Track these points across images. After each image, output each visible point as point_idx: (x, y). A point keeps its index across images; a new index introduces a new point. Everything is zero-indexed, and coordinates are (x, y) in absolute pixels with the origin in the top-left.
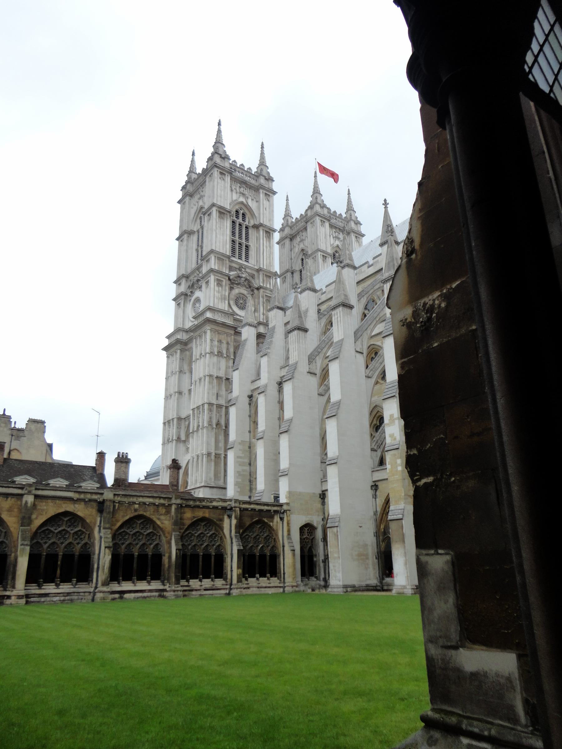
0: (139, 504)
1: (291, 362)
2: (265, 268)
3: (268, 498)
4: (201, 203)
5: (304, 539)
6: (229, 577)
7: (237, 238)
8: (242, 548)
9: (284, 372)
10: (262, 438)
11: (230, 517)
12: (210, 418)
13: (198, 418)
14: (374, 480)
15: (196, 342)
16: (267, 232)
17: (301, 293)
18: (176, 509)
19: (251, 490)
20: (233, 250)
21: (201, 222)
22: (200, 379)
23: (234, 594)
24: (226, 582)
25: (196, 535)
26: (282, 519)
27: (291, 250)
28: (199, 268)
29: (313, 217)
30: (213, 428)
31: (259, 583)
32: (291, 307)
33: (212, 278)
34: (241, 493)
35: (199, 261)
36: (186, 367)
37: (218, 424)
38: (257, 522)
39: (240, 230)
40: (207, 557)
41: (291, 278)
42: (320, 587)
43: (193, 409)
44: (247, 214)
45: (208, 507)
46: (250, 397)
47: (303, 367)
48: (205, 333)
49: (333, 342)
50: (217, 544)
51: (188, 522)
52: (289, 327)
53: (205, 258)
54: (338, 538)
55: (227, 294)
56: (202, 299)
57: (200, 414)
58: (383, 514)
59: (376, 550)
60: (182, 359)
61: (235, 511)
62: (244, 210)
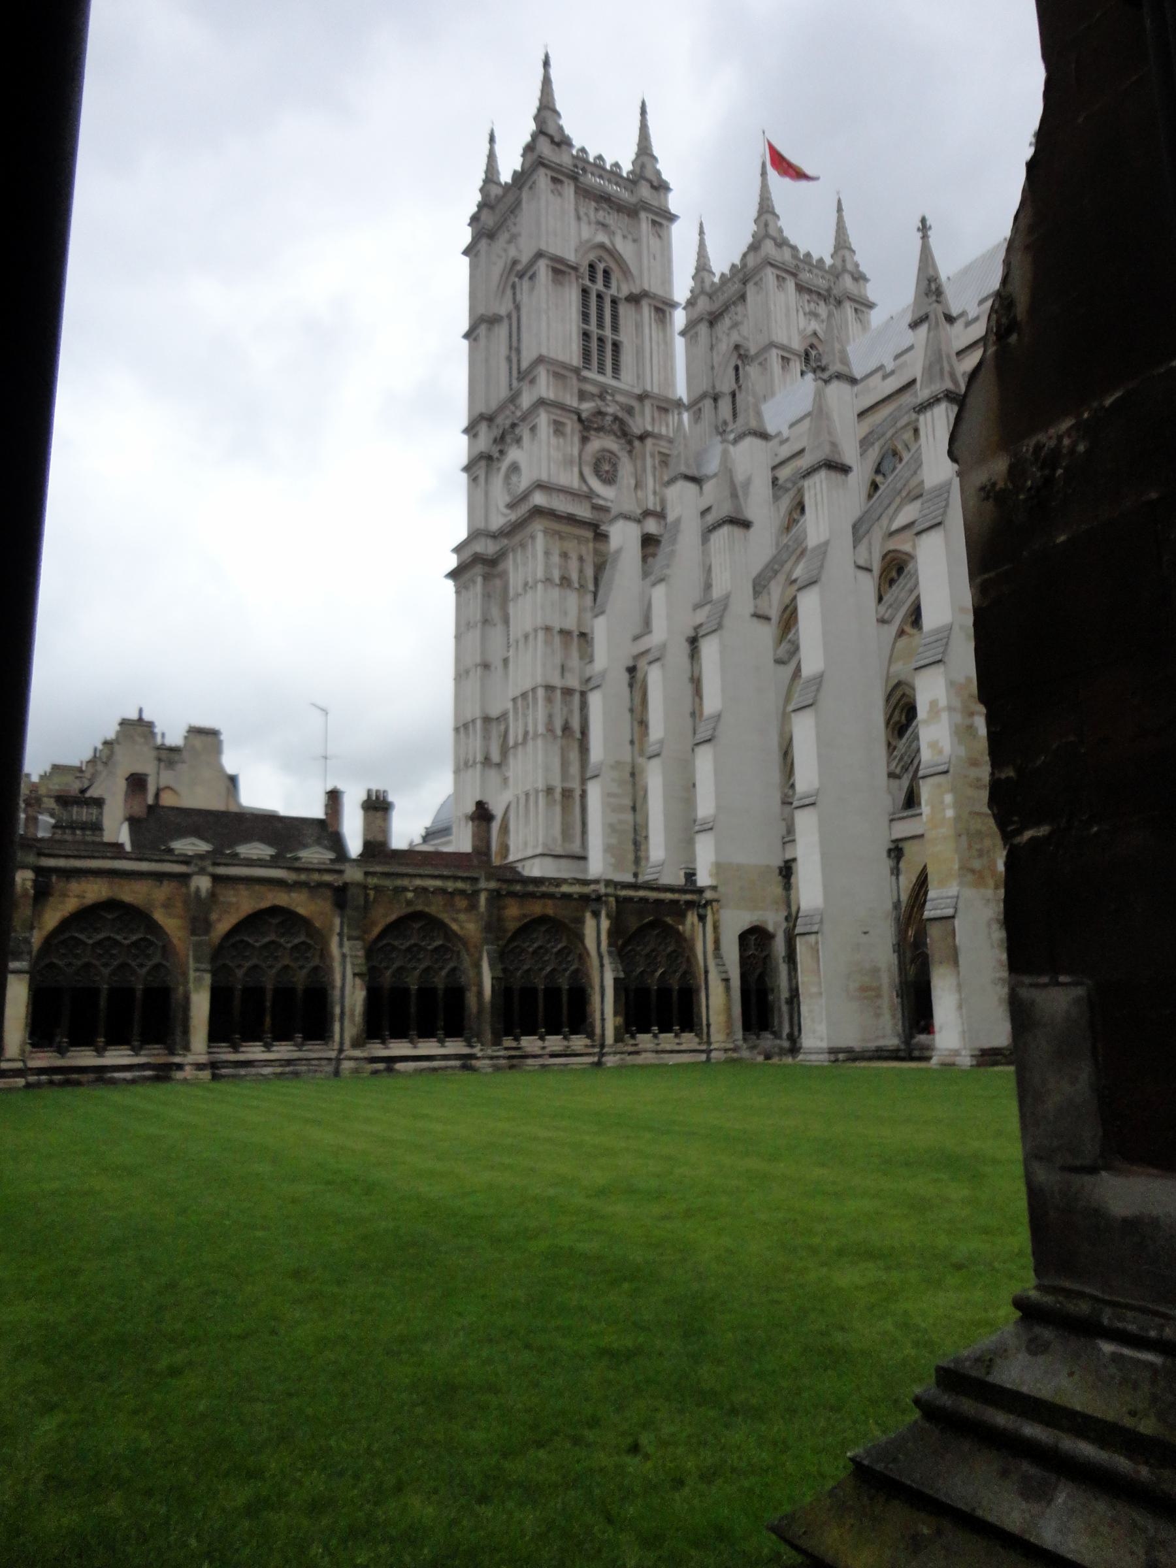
0: (413, 891)
1: (717, 593)
2: (656, 390)
3: (676, 878)
4: (512, 252)
5: (749, 957)
6: (598, 1031)
7: (593, 327)
8: (622, 975)
9: (701, 616)
10: (658, 755)
11: (596, 915)
12: (550, 717)
13: (525, 715)
14: (897, 835)
15: (515, 560)
16: (658, 310)
17: (735, 442)
18: (487, 899)
19: (637, 861)
20: (586, 355)
21: (514, 294)
22: (526, 637)
23: (609, 1065)
24: (593, 1041)
25: (531, 950)
26: (702, 918)
27: (712, 348)
28: (514, 398)
29: (758, 269)
30: (555, 737)
31: (658, 1044)
32: (715, 475)
33: (543, 419)
34: (618, 866)
35: (515, 383)
36: (495, 612)
37: (566, 728)
38: (652, 925)
39: (600, 309)
40: (553, 993)
41: (714, 411)
42: (782, 1052)
43: (514, 700)
45: (551, 896)
46: (632, 670)
47: (743, 604)
48: (533, 537)
49: (806, 547)
50: (573, 968)
51: (512, 926)
52: (711, 518)
53: (525, 376)
55: (576, 452)
56: (524, 466)
57: (528, 708)
58: (913, 907)
59: (897, 980)
60: (487, 596)
61: (606, 903)
62: (605, 261)
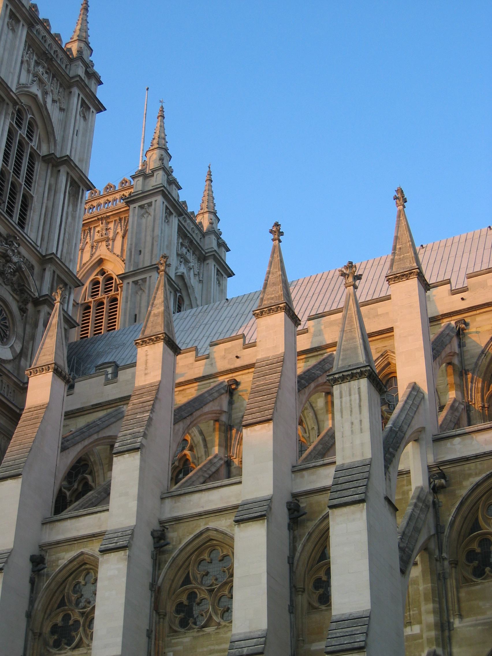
44: (37, 125)
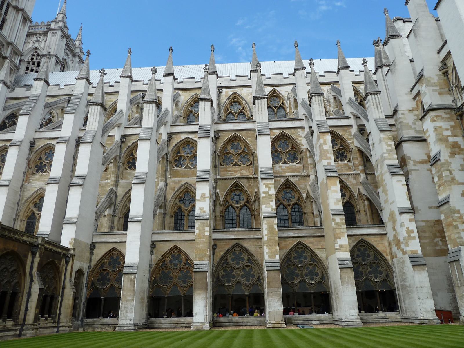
14: (152, 240)
16: (24, 18)
54: (135, 283)
